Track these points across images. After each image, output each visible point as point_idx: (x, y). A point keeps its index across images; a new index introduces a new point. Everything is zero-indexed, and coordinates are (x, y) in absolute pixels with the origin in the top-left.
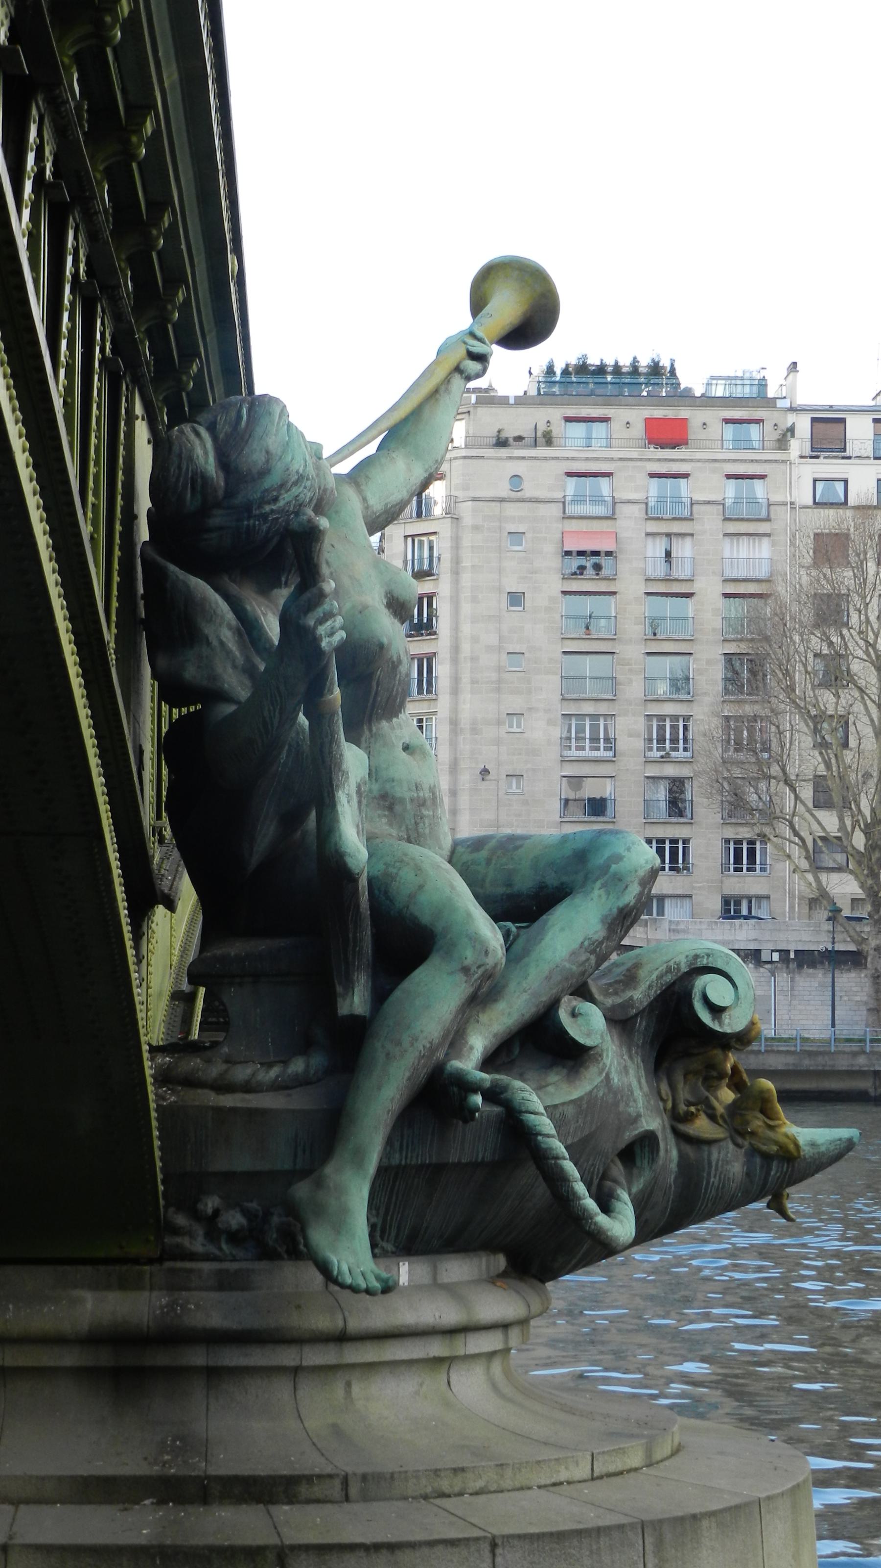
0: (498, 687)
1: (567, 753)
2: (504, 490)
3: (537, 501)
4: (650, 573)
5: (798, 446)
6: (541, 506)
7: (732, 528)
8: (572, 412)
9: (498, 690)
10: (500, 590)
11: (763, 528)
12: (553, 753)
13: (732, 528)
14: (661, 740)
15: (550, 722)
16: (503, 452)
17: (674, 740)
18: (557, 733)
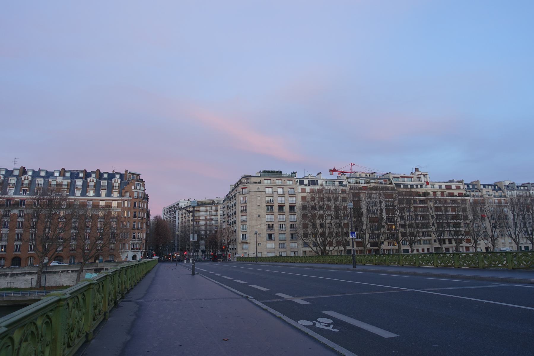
0: (256, 220)
1: (267, 230)
2: (256, 190)
3: (262, 191)
4: (279, 202)
5: (298, 183)
6: (263, 192)
7: (290, 196)
8: (265, 178)
9: (257, 220)
10: (256, 205)
11: (294, 196)
12: (265, 230)
13: (290, 196)
14: (269, 228)
15: (265, 225)
16: (256, 184)
17: (271, 228)
18: (266, 227)
